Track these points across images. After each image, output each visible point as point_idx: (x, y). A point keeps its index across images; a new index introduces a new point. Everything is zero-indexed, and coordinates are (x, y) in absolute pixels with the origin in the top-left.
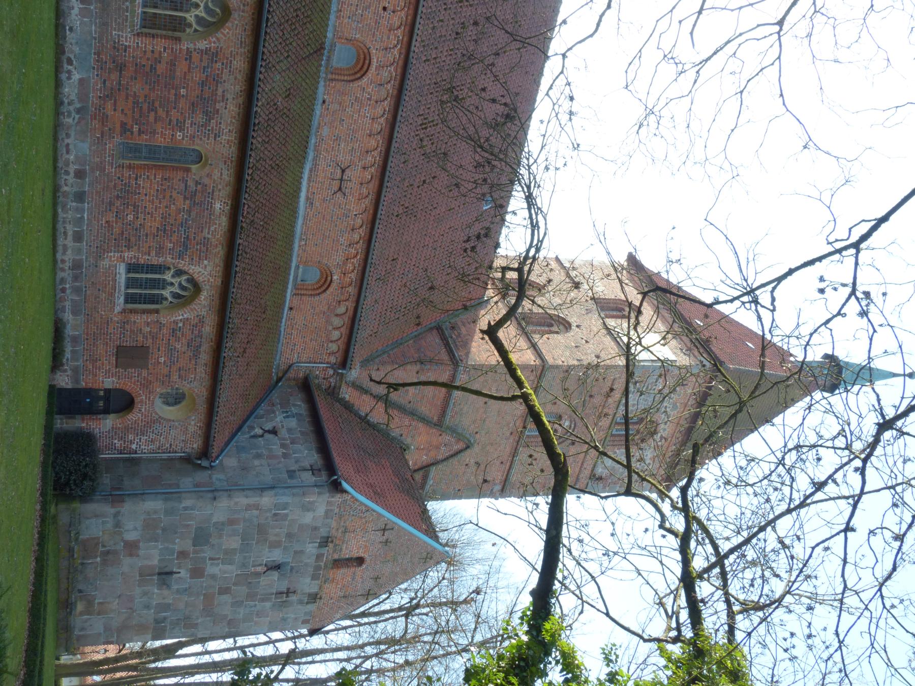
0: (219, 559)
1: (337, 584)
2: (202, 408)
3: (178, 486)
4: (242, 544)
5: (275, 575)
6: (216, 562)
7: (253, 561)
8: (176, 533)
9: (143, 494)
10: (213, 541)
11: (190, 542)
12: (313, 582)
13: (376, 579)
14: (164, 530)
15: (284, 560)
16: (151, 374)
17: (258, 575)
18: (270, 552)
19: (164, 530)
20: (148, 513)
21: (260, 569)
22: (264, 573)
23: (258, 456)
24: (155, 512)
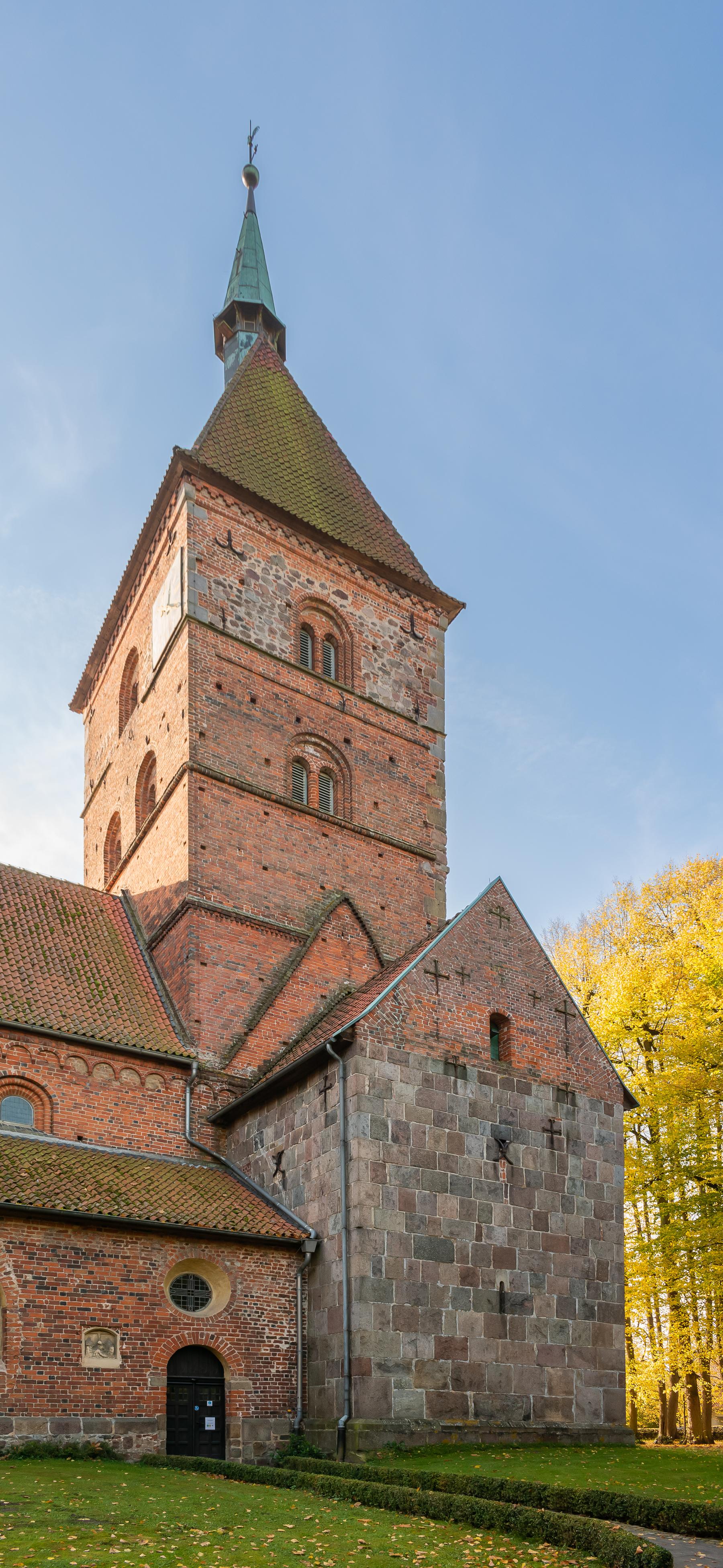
0: (479, 1228)
1: (541, 1057)
2: (207, 1251)
3: (341, 1282)
4: (451, 1192)
5: (517, 1149)
6: (484, 1231)
7: (487, 1177)
8: (424, 1286)
9: (349, 1331)
10: (443, 1233)
11: (443, 1267)
12: (534, 1092)
13: (535, 998)
14: (417, 1302)
15: (488, 1131)
16: (136, 1321)
17: (513, 1173)
18: (470, 1152)
19: (417, 1302)
20: (384, 1324)
21: (503, 1169)
22: (510, 1163)
23: (307, 1173)
24: (382, 1314)
